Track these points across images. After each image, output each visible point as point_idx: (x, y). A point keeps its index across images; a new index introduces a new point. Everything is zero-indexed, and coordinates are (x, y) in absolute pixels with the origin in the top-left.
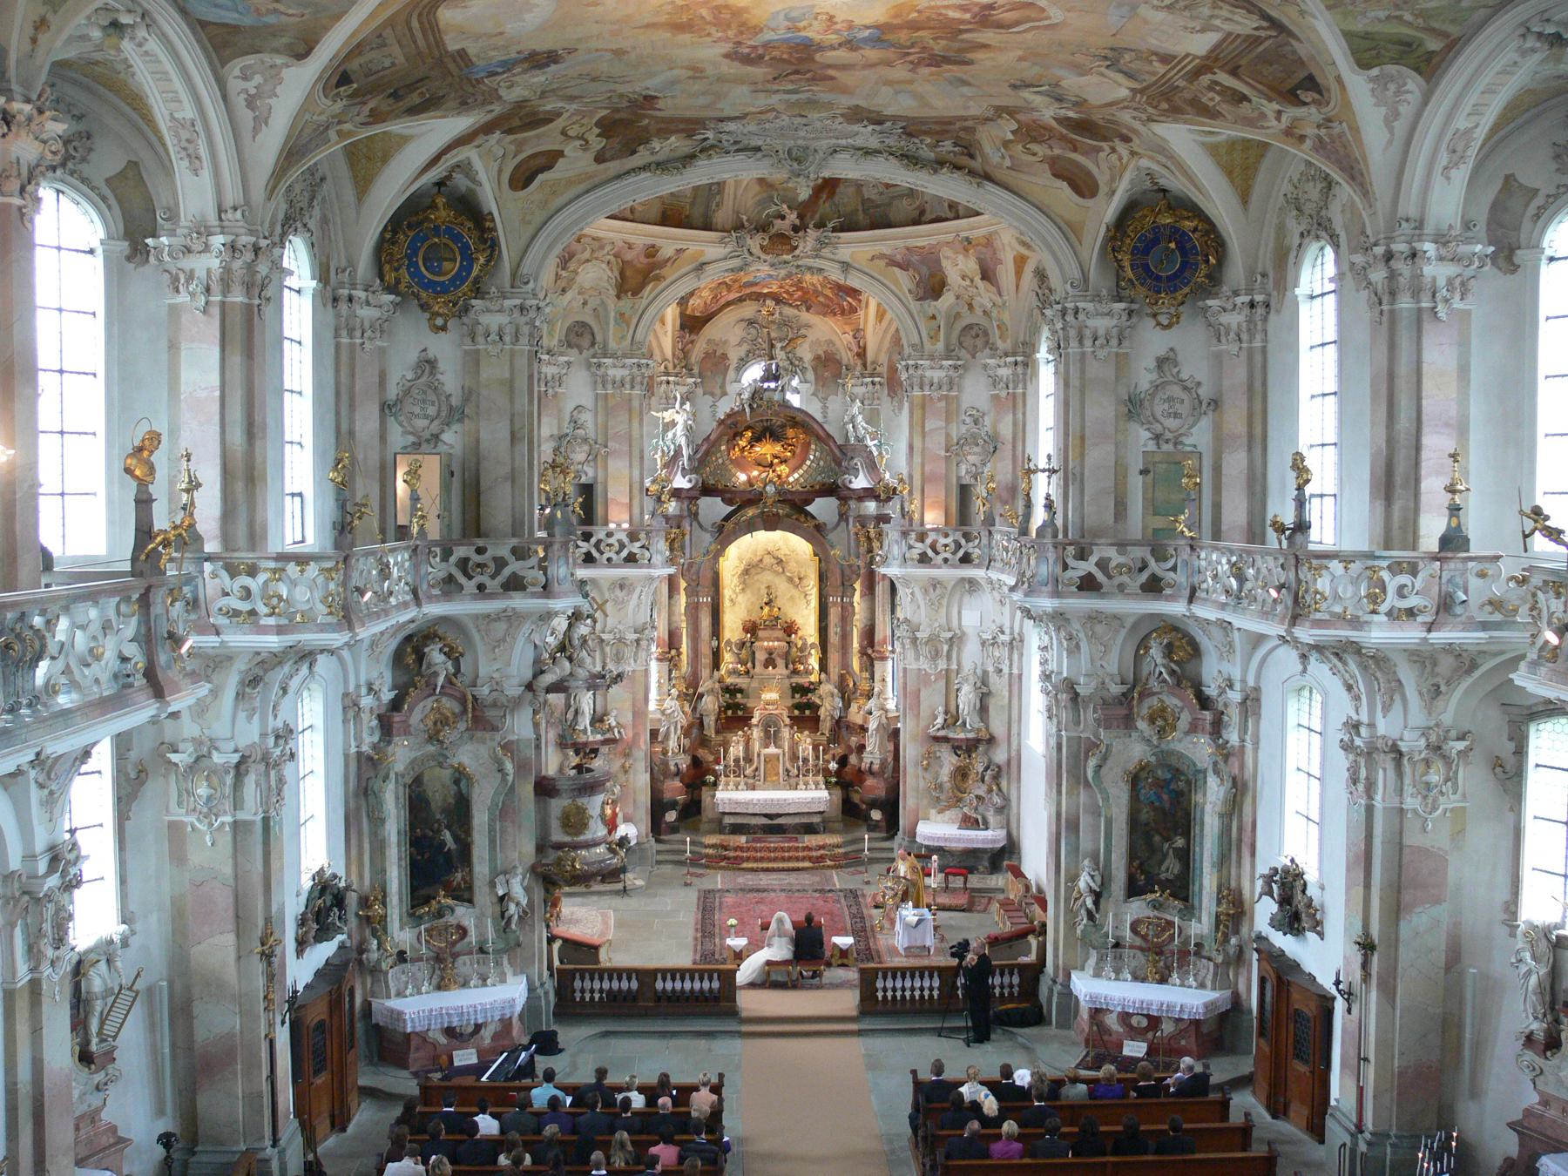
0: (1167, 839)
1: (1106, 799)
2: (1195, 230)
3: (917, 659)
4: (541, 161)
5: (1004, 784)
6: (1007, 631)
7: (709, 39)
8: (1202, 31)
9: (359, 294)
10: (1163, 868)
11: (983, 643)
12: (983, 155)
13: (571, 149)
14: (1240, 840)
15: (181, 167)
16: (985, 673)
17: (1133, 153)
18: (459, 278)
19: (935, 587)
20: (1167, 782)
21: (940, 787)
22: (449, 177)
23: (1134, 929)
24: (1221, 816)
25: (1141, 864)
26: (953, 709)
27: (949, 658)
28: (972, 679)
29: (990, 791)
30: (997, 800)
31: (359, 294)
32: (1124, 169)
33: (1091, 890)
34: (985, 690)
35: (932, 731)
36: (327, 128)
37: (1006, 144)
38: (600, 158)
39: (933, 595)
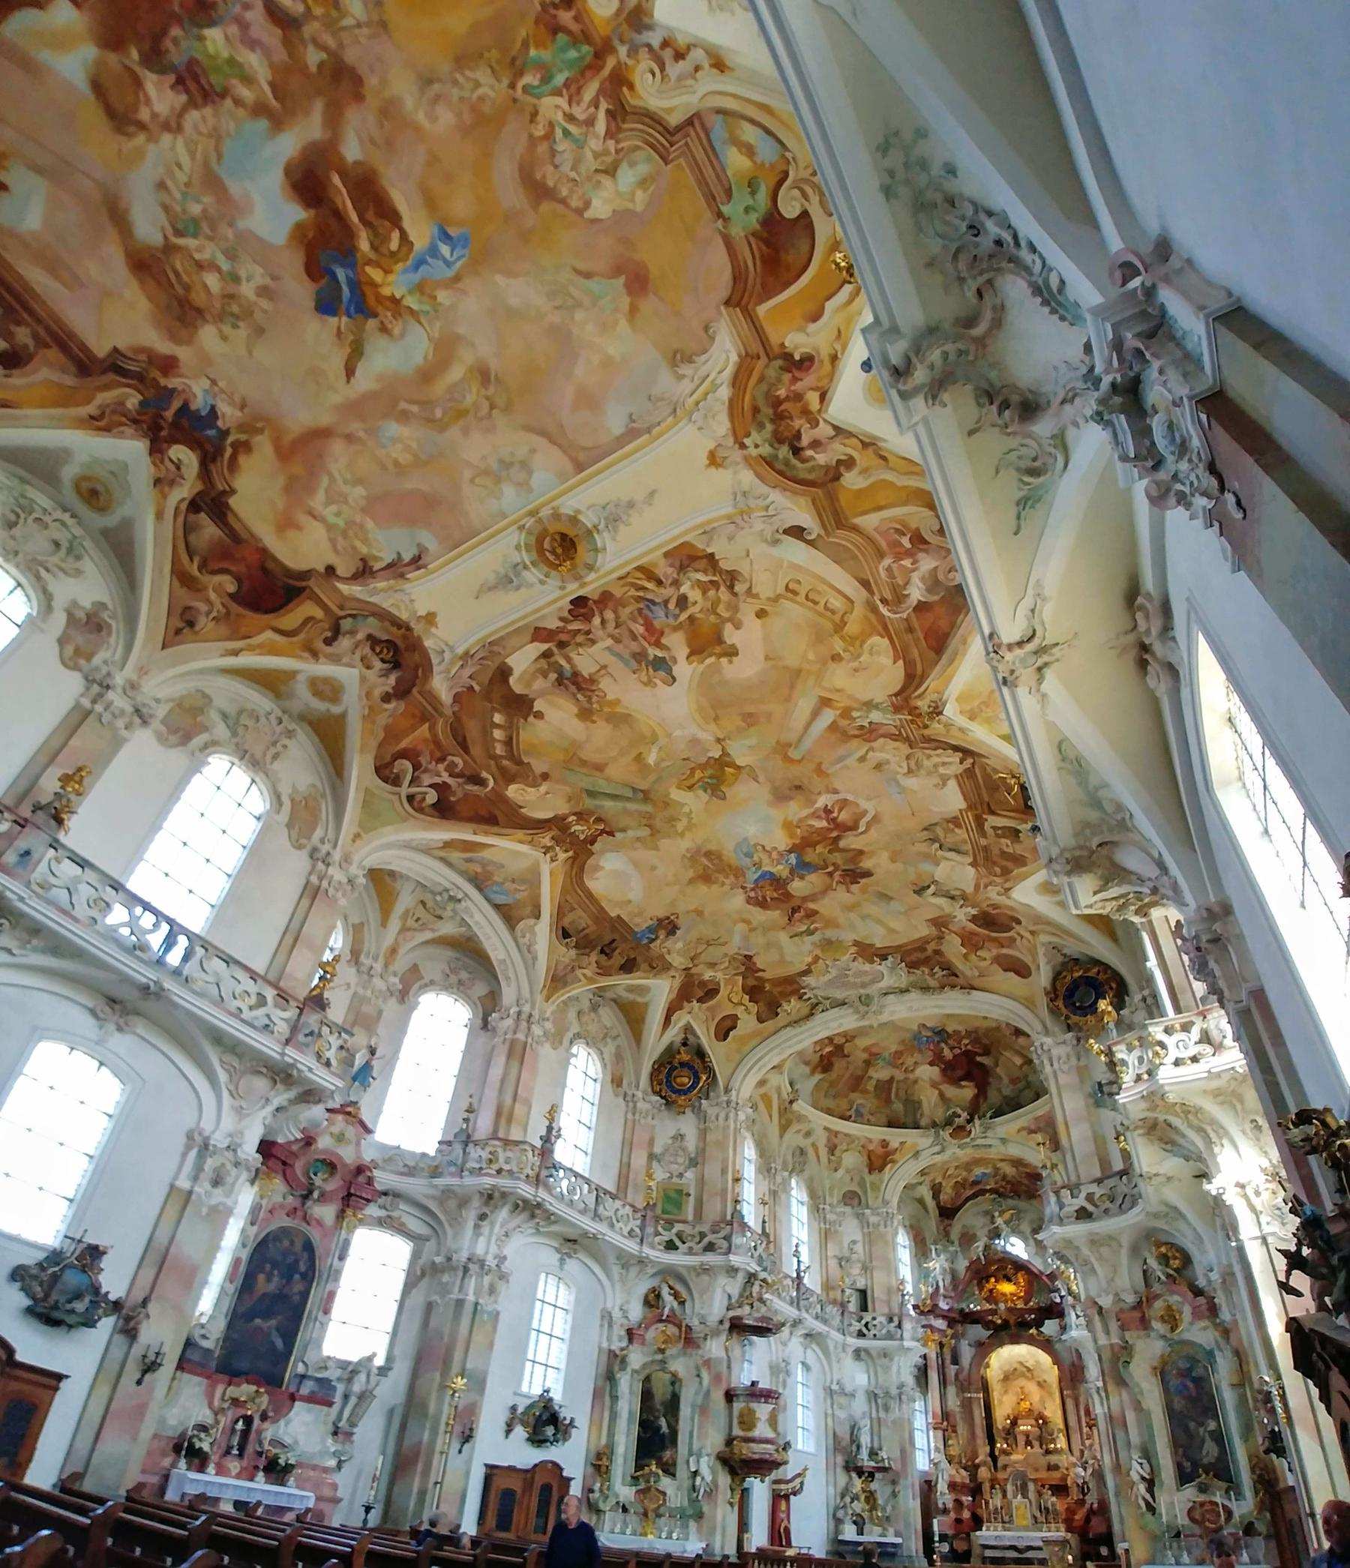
2: (1098, 973)
4: (728, 1023)
7: (726, 888)
8: (944, 784)
9: (639, 1094)
12: (962, 973)
13: (740, 1011)
15: (503, 984)
17: (1032, 933)
18: (693, 1087)
22: (686, 1038)
31: (639, 1094)
32: (1035, 947)
36: (573, 969)
37: (966, 956)
38: (761, 1020)
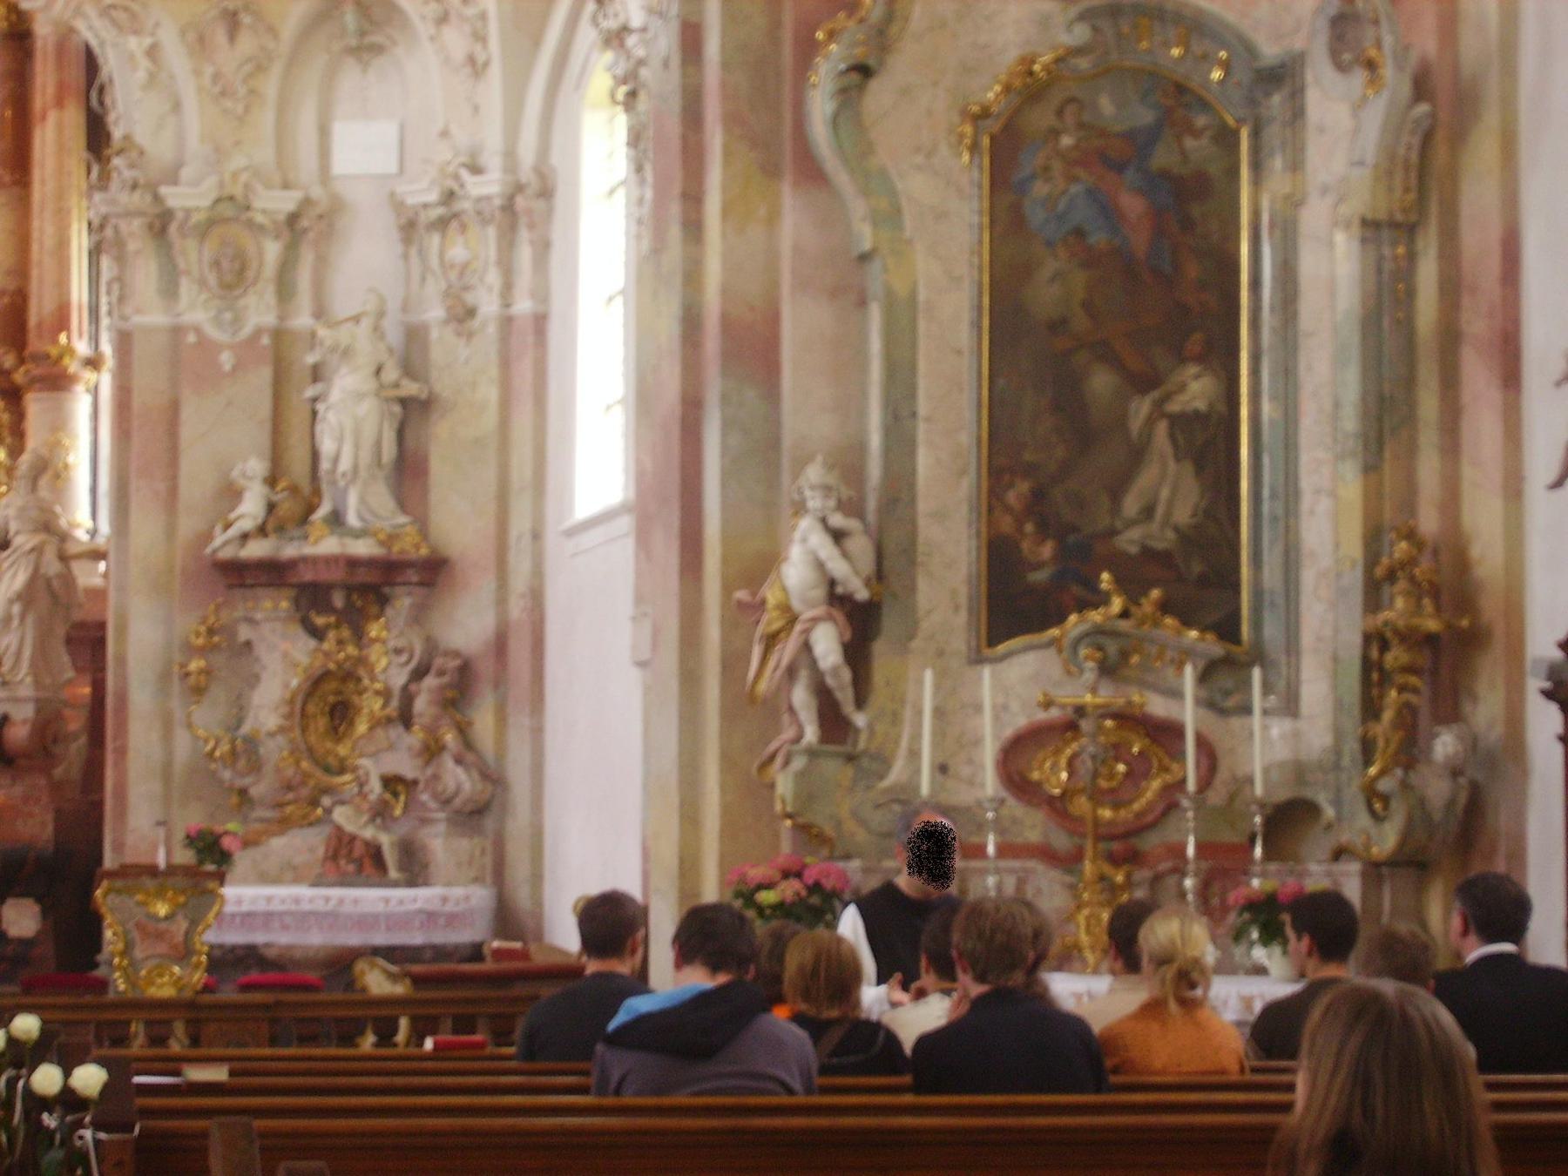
0: (1145, 382)
1: (890, 217)
3: (170, 290)
5: (483, 721)
6: (493, 162)
10: (1131, 505)
11: (409, 229)
14: (1450, 338)
16: (415, 336)
19: (232, 21)
20: (1141, 142)
21: (246, 752)
23: (1016, 780)
24: (1371, 228)
25: (1038, 496)
26: (298, 466)
27: (284, 289)
28: (365, 348)
29: (431, 751)
30: (457, 778)
33: (837, 599)
34: (410, 388)
35: (222, 544)
39: (231, 57)
